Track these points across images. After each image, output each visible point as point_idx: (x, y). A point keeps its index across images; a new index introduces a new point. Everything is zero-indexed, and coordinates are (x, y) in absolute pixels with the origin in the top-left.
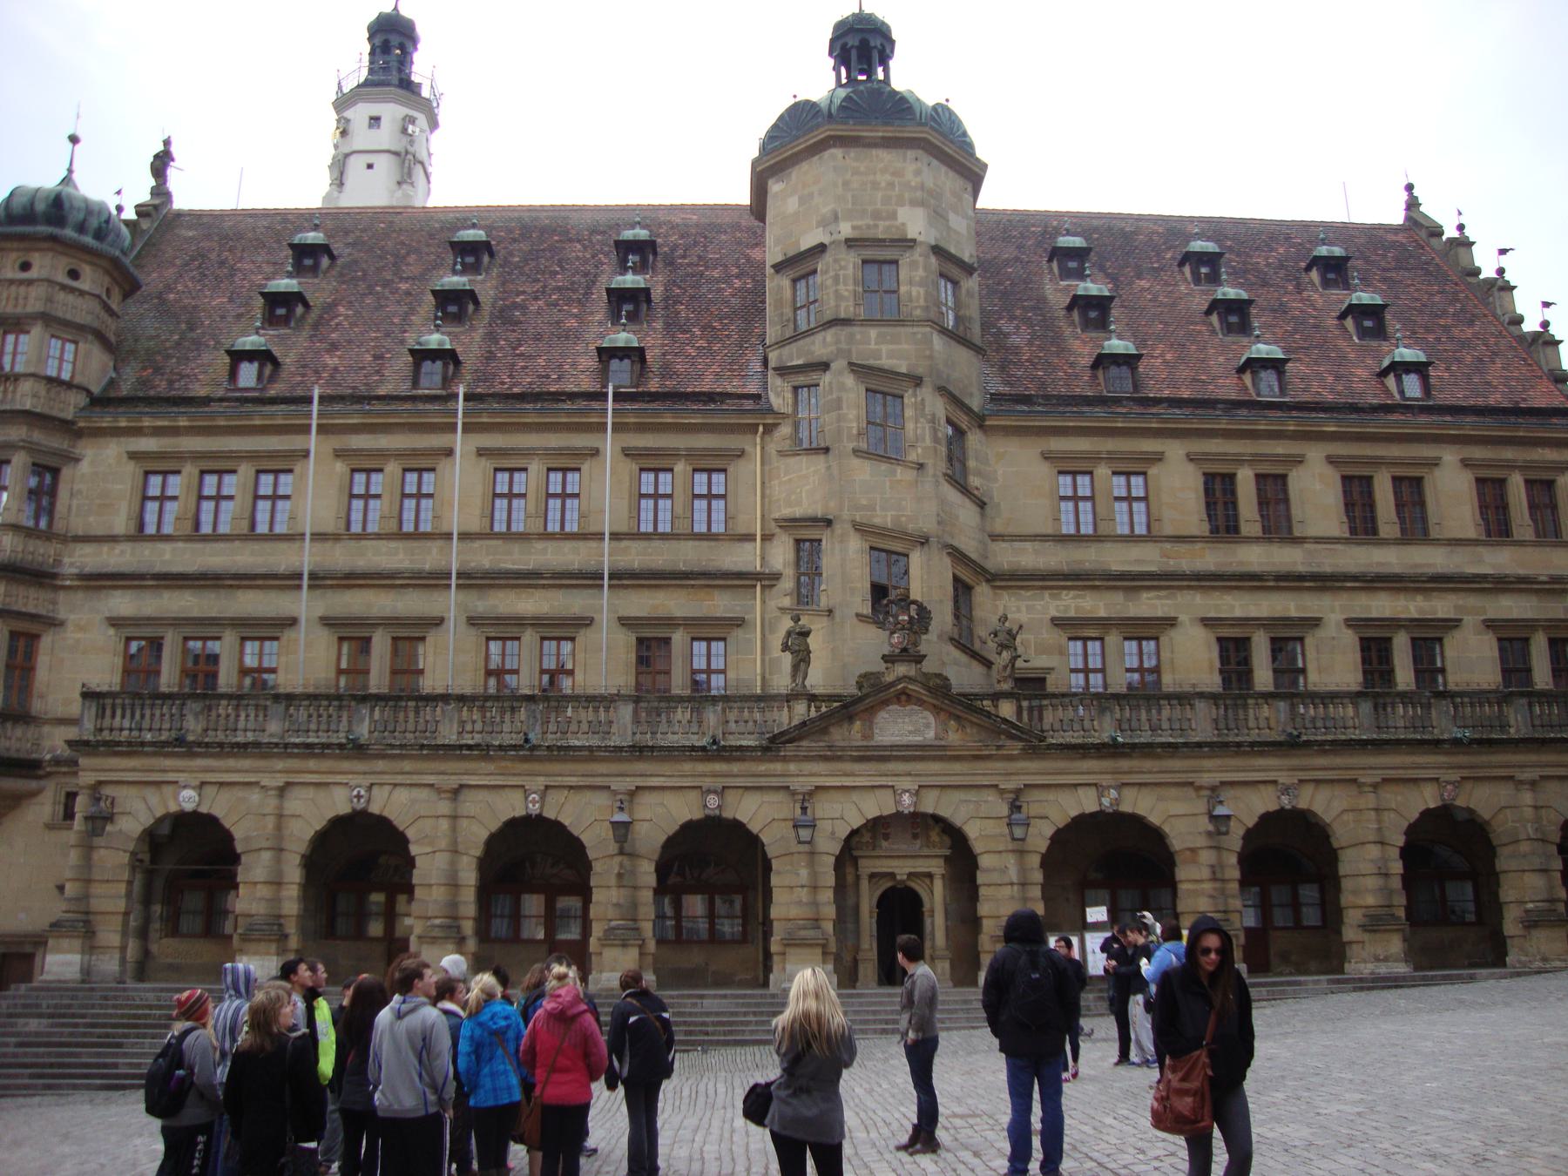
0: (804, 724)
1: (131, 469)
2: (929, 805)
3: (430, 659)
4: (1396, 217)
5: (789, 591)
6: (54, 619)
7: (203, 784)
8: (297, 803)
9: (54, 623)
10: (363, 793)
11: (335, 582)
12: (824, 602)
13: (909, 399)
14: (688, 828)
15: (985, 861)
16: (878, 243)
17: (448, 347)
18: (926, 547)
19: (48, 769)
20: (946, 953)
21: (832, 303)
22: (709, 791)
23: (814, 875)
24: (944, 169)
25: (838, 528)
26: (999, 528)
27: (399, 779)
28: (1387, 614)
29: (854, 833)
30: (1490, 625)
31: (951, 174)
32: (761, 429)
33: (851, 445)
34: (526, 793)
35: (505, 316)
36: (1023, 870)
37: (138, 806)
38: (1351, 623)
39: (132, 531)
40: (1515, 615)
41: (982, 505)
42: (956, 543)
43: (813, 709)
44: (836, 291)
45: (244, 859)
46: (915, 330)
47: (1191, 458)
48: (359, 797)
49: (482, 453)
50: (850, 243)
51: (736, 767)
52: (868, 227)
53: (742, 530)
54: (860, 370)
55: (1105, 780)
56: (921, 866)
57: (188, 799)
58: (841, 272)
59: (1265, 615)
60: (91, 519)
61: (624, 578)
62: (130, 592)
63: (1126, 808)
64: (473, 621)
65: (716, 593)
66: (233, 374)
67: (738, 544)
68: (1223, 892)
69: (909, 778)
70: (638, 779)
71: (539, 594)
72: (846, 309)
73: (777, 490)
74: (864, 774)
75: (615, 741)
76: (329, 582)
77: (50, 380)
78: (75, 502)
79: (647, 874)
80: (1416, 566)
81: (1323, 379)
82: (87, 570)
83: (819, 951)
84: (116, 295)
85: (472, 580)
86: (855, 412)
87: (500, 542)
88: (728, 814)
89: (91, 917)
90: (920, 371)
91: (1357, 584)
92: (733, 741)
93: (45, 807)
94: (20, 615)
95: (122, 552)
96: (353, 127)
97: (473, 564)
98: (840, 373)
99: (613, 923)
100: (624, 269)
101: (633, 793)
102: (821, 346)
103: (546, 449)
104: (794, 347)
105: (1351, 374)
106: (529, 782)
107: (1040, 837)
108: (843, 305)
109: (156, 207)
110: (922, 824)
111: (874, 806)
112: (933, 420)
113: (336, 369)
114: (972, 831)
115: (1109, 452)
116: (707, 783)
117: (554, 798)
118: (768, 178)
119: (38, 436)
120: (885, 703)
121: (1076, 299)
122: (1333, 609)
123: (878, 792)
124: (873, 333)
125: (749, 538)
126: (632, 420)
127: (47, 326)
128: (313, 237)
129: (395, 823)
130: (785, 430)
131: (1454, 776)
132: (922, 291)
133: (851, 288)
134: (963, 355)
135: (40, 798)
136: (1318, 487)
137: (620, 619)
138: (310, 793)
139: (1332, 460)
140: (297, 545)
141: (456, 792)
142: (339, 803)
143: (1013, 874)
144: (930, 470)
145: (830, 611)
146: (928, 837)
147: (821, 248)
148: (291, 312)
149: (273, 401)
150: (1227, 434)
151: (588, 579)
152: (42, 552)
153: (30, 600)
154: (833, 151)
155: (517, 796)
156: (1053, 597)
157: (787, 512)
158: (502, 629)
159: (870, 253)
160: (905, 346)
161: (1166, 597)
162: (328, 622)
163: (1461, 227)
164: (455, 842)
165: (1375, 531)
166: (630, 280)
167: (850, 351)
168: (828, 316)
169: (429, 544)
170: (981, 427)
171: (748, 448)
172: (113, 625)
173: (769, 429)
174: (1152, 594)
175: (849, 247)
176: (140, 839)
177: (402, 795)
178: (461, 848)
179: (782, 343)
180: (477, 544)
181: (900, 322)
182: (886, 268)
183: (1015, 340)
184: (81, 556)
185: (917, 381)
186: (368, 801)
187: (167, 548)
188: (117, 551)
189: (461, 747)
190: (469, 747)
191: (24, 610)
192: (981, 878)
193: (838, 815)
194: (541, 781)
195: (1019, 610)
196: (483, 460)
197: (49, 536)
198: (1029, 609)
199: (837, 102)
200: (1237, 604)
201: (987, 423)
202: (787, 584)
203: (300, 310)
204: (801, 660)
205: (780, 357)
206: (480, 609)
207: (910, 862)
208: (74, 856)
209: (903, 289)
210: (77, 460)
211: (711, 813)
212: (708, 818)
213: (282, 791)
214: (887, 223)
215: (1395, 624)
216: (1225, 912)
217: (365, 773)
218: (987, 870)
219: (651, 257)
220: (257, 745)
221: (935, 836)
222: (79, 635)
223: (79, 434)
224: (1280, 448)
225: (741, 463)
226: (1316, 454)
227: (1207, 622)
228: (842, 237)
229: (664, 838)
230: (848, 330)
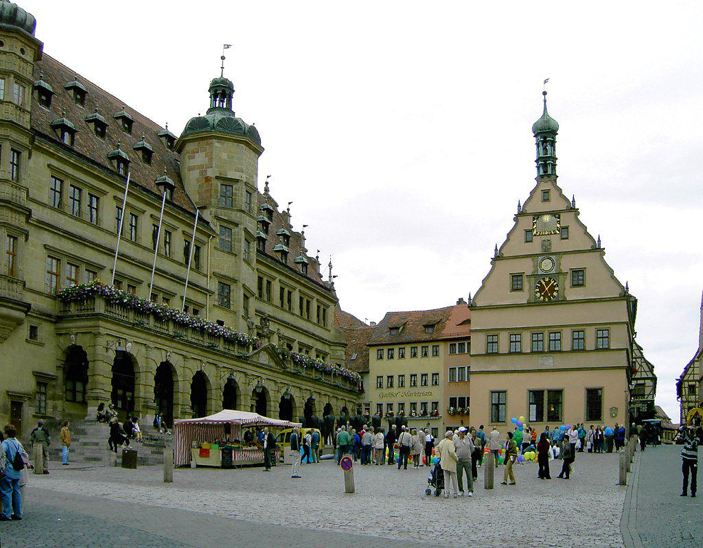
25: (238, 283)
27: (176, 351)
30: (316, 350)
50: (246, 184)
54: (246, 230)
57: (129, 347)
106: (205, 360)
116: (233, 367)
125: (206, 276)
147: (237, 181)
157: (217, 271)
172: (45, 248)
202: (216, 297)
222: (33, 248)
224: (293, 283)
230: (243, 215)
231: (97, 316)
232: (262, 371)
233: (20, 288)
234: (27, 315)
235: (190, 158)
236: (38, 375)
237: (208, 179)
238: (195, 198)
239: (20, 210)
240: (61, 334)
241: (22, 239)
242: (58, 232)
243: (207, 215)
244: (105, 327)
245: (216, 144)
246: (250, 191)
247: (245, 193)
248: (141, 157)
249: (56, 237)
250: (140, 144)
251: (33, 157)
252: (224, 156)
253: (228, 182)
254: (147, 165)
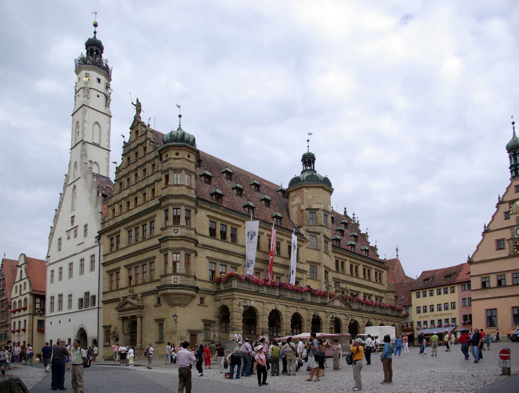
1: (208, 219)
12: (318, 279)
50: (324, 210)
53: (302, 261)
54: (325, 236)
57: (252, 304)
60: (201, 230)
62: (210, 251)
72: (323, 224)
95: (208, 240)
104: (311, 227)
124: (326, 229)
130: (308, 243)
135: (196, 298)
147: (318, 209)
172: (207, 258)
173: (306, 242)
184: (199, 239)
187: (216, 241)
222: (200, 259)
230: (322, 228)
231: (234, 290)
233: (192, 279)
234: (197, 293)
235: (292, 201)
236: (204, 321)
237: (302, 211)
238: (295, 222)
239: (191, 240)
240: (217, 300)
241: (193, 255)
243: (302, 231)
244: (237, 295)
245: (305, 191)
246: (327, 214)
247: (323, 216)
248: (264, 204)
250: (263, 197)
251: (199, 212)
252: (310, 196)
253: (313, 211)
254: (267, 208)
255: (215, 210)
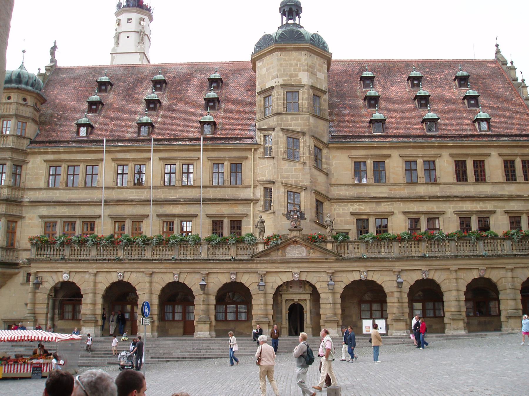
0: (262, 251)
1: (45, 166)
2: (303, 278)
3: (145, 228)
4: (491, 56)
5: (262, 205)
6: (22, 216)
7: (70, 272)
8: (100, 278)
9: (22, 218)
10: (121, 275)
11: (113, 203)
13: (301, 140)
14: (226, 285)
15: (322, 296)
16: (292, 86)
17: (149, 122)
18: (306, 191)
19: (21, 266)
20: (311, 325)
21: (276, 107)
22: (232, 274)
23: (266, 301)
24: (316, 57)
25: (276, 184)
26: (333, 182)
27: (133, 270)
28: (469, 209)
29: (279, 287)
31: (319, 58)
32: (253, 150)
33: (282, 157)
34: (174, 275)
35: (171, 108)
36: (334, 299)
37: (50, 279)
38: (456, 213)
39: (46, 187)
40: (516, 209)
41: (327, 174)
42: (317, 189)
43: (266, 246)
44: (277, 103)
45: (83, 296)
46: (304, 116)
47: (401, 156)
48: (120, 276)
49: (160, 159)
50: (282, 86)
51: (241, 266)
52: (288, 80)
55: (362, 269)
56: (302, 297)
57: (65, 277)
58: (279, 96)
59: (425, 210)
61: (207, 201)
62: (45, 207)
63: (369, 278)
64: (158, 216)
65: (238, 205)
66: (78, 132)
67: (245, 189)
68: (402, 306)
69: (297, 269)
70: (209, 270)
71: (180, 206)
72: (281, 109)
73: (258, 170)
74: (282, 268)
75: (202, 257)
76: (111, 203)
77: (18, 136)
78: (27, 177)
79: (213, 300)
80: (481, 192)
81: (452, 124)
82: (32, 200)
83: (267, 325)
84: (39, 103)
85: (158, 202)
86: (283, 145)
87: (167, 189)
88: (238, 281)
89: (36, 315)
90: (305, 130)
91: (458, 199)
92: (239, 258)
93: (20, 278)
94: (10, 215)
96: (122, 23)
97: (158, 197)
98: (278, 132)
99: (201, 316)
100: (210, 89)
101: (208, 274)
102: (272, 121)
103: (182, 158)
105: (464, 122)
107: (340, 288)
108: (279, 108)
109: (51, 67)
110: (303, 283)
111: (286, 278)
112: (309, 147)
113: (112, 129)
114: (318, 286)
115: (371, 155)
116: (231, 271)
117: (183, 276)
118: (257, 60)
119: (15, 156)
120: (289, 244)
121: (366, 97)
122: (450, 208)
123: (287, 273)
124: (289, 117)
125: (250, 187)
126: (210, 148)
127: (16, 118)
128: (105, 79)
129: (132, 284)
130: (261, 150)
131: (484, 267)
132: (306, 102)
133: (282, 102)
134: (321, 123)
135: (18, 275)
136: (446, 165)
137: (206, 215)
138: (105, 275)
139: (451, 155)
140: (100, 191)
141: (151, 274)
142: (114, 278)
143: (331, 300)
144: (308, 164)
145: (274, 213)
146: (305, 287)
147: (273, 88)
148: (97, 108)
149: (91, 141)
150: (414, 147)
151: (196, 201)
152: (17, 194)
153: (14, 211)
154: (276, 53)
155: (171, 275)
156: (351, 205)
158: (168, 218)
159: (289, 89)
160: (301, 122)
161: (390, 205)
162: (111, 217)
163: (512, 62)
164: (151, 290)
165: (466, 180)
166: (212, 94)
167: (281, 124)
168: (275, 112)
169: (143, 190)
170: (327, 147)
171: (249, 156)
172: (41, 218)
173: (256, 150)
174: (386, 203)
175: (282, 87)
176: (51, 290)
177: (134, 275)
178: (153, 292)
179: (261, 120)
180: (159, 190)
181: (299, 114)
182: (294, 94)
183: (344, 113)
185: (304, 134)
186: (123, 277)
187: (57, 192)
188: (41, 193)
189: (152, 260)
190: (155, 260)
191: (12, 214)
192: (321, 301)
193: (274, 281)
194: (179, 270)
195: (339, 210)
196: (161, 161)
197: (19, 189)
198: (343, 209)
199: (278, 35)
200: (415, 206)
201: (329, 146)
202: (261, 202)
203: (100, 106)
204: (261, 231)
205: (259, 125)
206: (161, 212)
207: (299, 296)
208: (30, 296)
209: (300, 102)
210: (28, 163)
211: (233, 280)
212: (232, 282)
213: (96, 274)
214: (295, 78)
215: (472, 213)
216: (403, 313)
217: (122, 268)
218: (323, 299)
219: (220, 84)
220: (88, 260)
221: (307, 287)
222: (29, 221)
223: (28, 154)
224: (433, 152)
225: (247, 161)
226: (445, 153)
227: (405, 213)
228: (279, 84)
229: (218, 288)
230: (280, 117)
232: (291, 265)
242: (50, 204)
249: (51, 208)
255: (54, 150)
